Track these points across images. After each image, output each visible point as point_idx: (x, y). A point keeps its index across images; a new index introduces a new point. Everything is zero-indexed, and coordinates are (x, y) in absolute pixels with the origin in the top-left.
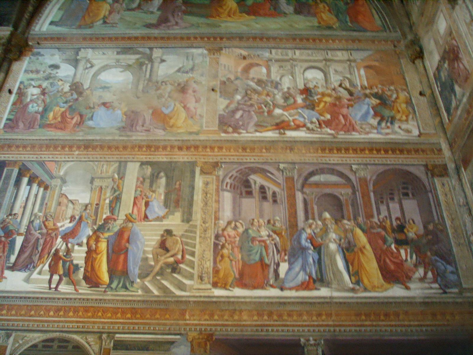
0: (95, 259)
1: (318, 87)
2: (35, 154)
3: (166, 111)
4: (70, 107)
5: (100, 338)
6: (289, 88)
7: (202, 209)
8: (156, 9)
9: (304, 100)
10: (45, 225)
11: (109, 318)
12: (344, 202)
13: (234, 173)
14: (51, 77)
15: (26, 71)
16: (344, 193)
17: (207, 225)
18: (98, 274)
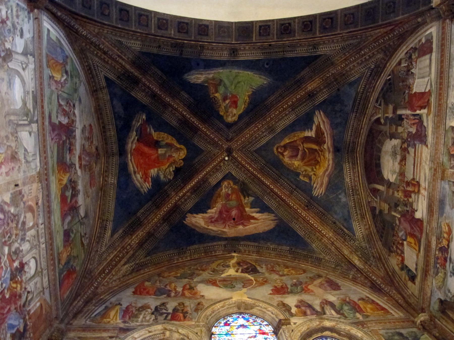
9: (17, 268)
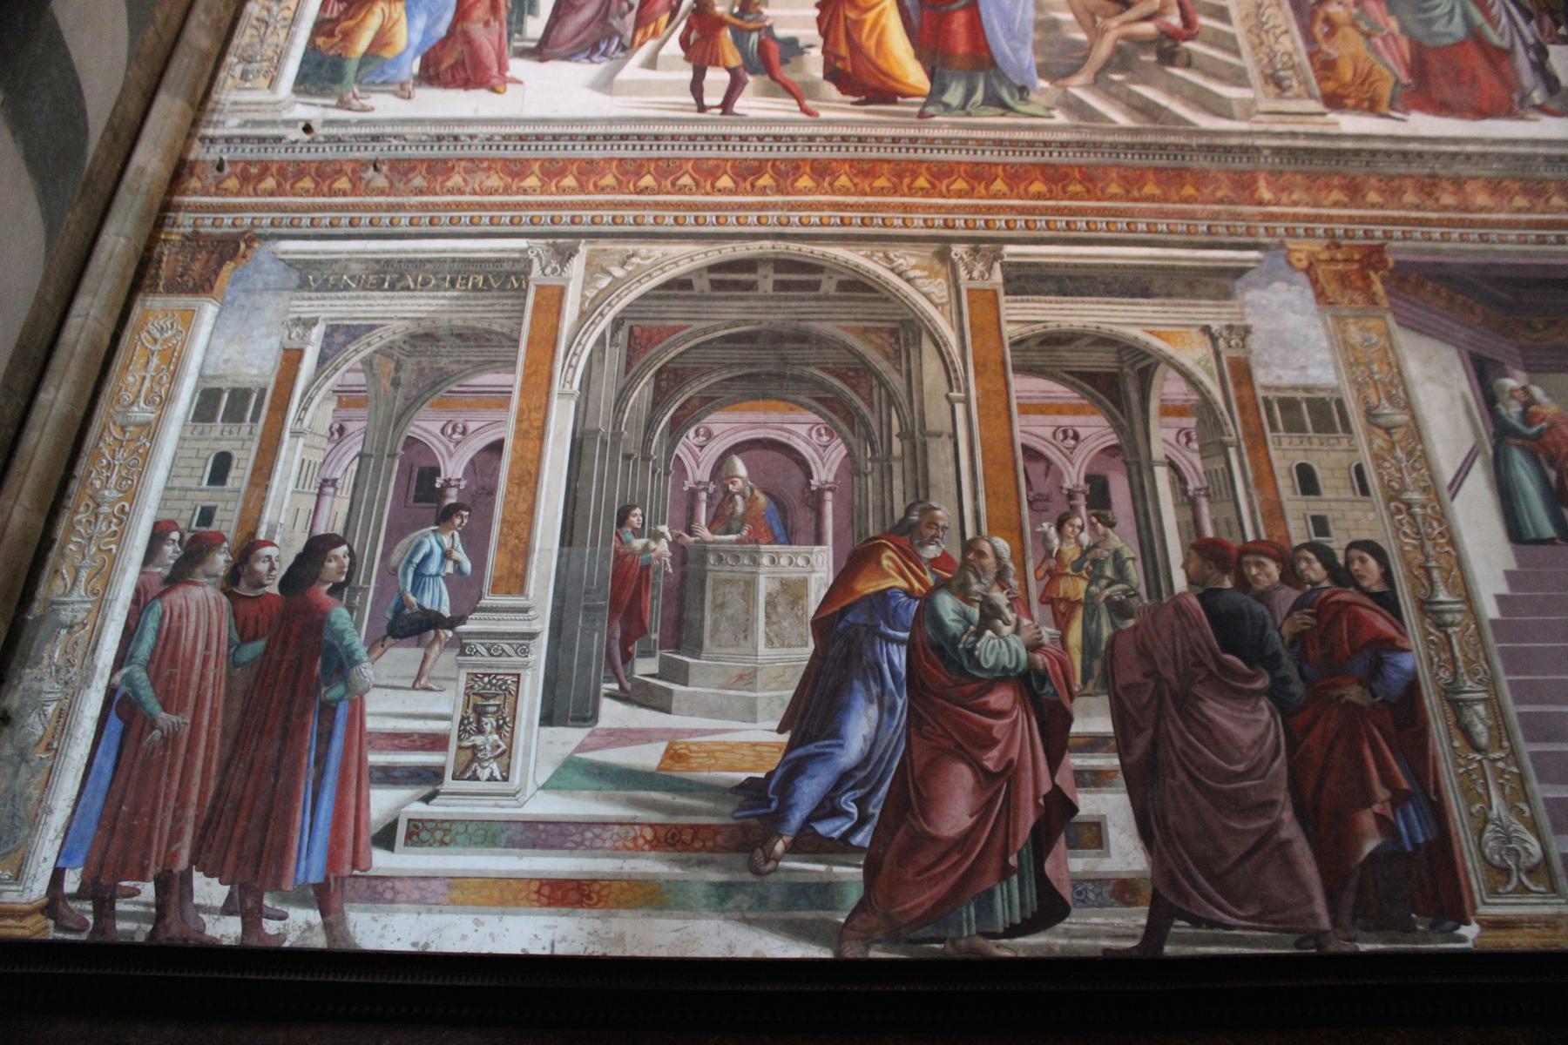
0: (859, 24)
5: (944, 256)
11: (960, 194)
18: (881, 63)
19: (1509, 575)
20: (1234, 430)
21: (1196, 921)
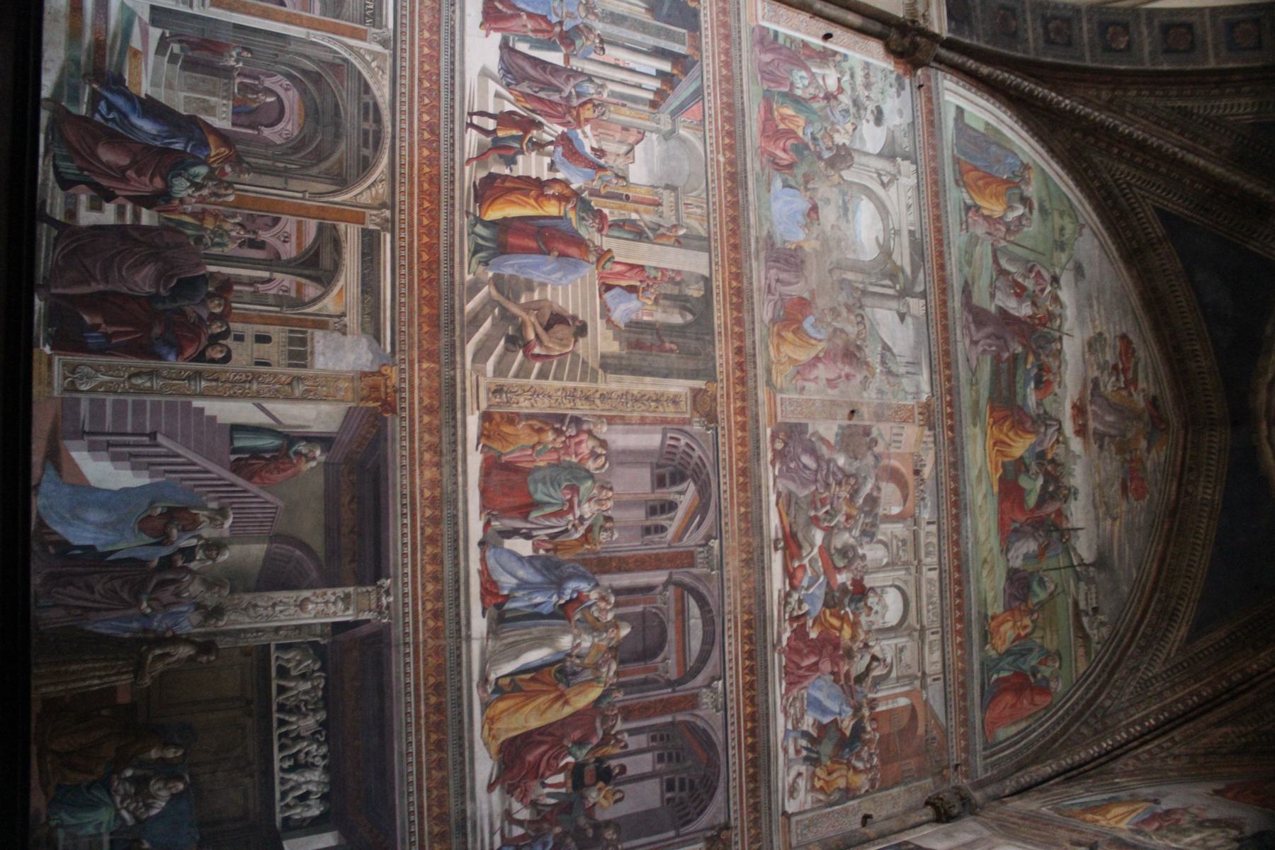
0: (527, 196)
1: (868, 615)
2: (714, 83)
3: (808, 324)
4: (806, 147)
5: (383, 206)
6: (863, 557)
7: (627, 393)
8: (1001, 304)
10: (585, 103)
12: (650, 664)
13: (698, 452)
14: (858, 110)
15: (867, 66)
16: (668, 664)
17: (598, 402)
18: (501, 200)
19: (213, 418)
20: (289, 313)
21: (56, 239)
